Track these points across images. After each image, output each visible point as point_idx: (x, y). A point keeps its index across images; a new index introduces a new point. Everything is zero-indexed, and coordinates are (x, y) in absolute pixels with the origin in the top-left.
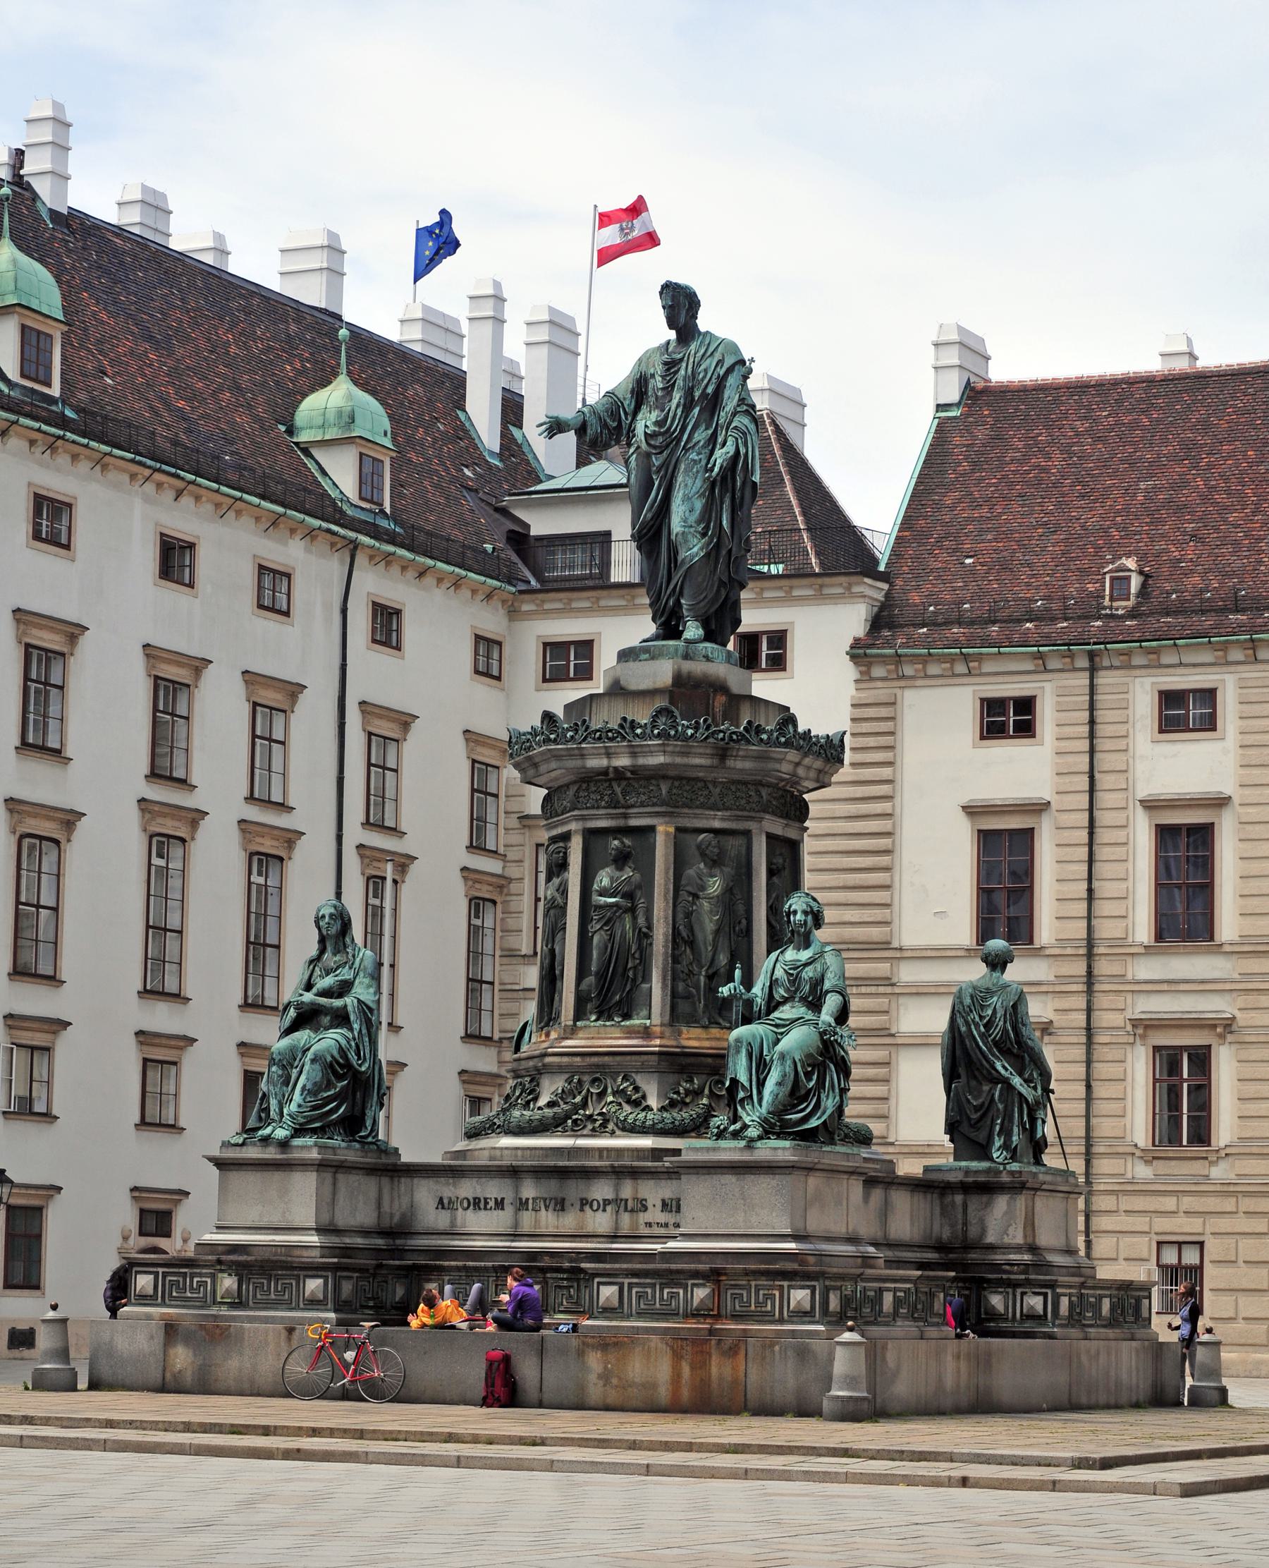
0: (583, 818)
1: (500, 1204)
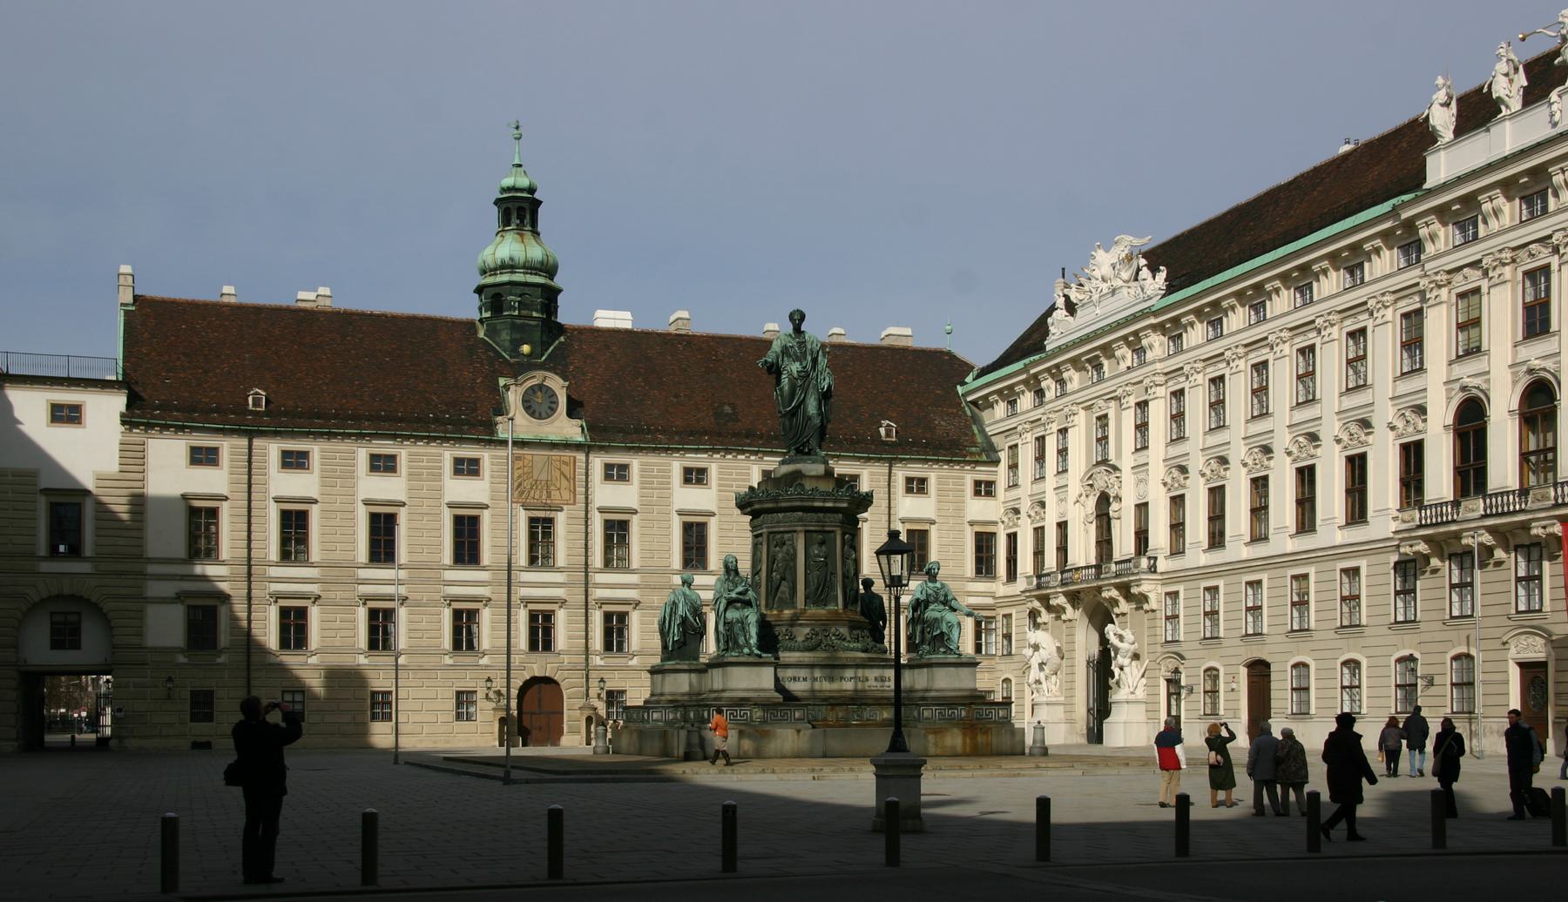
0: (806, 526)
1: (805, 679)
